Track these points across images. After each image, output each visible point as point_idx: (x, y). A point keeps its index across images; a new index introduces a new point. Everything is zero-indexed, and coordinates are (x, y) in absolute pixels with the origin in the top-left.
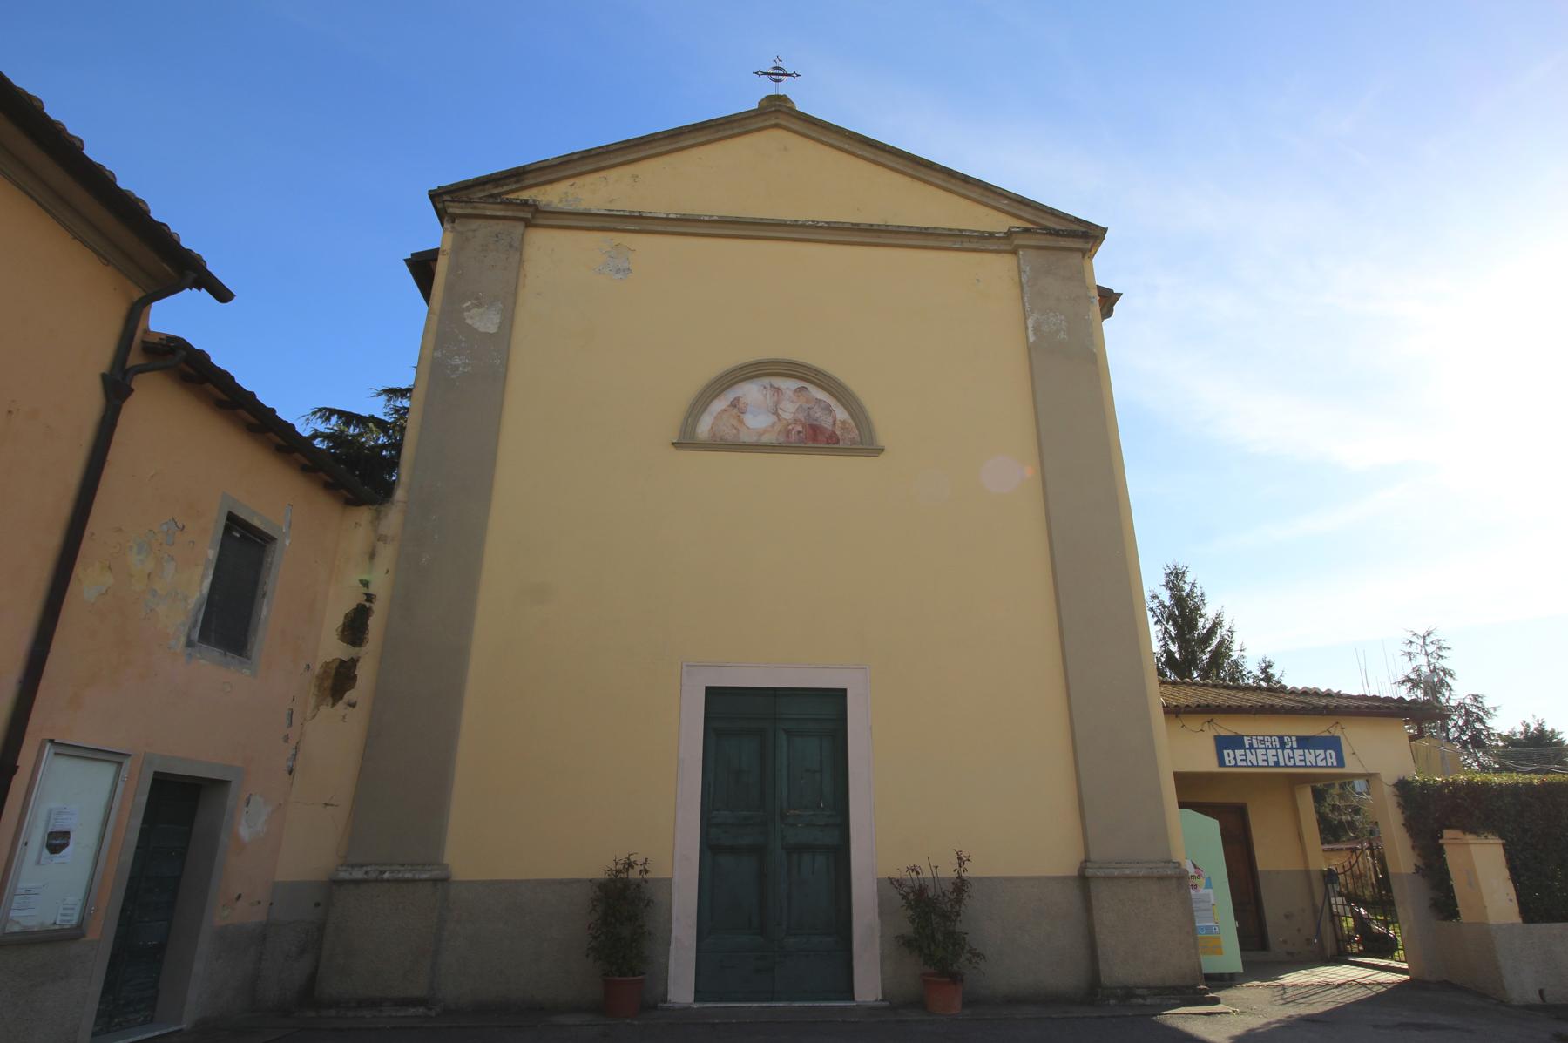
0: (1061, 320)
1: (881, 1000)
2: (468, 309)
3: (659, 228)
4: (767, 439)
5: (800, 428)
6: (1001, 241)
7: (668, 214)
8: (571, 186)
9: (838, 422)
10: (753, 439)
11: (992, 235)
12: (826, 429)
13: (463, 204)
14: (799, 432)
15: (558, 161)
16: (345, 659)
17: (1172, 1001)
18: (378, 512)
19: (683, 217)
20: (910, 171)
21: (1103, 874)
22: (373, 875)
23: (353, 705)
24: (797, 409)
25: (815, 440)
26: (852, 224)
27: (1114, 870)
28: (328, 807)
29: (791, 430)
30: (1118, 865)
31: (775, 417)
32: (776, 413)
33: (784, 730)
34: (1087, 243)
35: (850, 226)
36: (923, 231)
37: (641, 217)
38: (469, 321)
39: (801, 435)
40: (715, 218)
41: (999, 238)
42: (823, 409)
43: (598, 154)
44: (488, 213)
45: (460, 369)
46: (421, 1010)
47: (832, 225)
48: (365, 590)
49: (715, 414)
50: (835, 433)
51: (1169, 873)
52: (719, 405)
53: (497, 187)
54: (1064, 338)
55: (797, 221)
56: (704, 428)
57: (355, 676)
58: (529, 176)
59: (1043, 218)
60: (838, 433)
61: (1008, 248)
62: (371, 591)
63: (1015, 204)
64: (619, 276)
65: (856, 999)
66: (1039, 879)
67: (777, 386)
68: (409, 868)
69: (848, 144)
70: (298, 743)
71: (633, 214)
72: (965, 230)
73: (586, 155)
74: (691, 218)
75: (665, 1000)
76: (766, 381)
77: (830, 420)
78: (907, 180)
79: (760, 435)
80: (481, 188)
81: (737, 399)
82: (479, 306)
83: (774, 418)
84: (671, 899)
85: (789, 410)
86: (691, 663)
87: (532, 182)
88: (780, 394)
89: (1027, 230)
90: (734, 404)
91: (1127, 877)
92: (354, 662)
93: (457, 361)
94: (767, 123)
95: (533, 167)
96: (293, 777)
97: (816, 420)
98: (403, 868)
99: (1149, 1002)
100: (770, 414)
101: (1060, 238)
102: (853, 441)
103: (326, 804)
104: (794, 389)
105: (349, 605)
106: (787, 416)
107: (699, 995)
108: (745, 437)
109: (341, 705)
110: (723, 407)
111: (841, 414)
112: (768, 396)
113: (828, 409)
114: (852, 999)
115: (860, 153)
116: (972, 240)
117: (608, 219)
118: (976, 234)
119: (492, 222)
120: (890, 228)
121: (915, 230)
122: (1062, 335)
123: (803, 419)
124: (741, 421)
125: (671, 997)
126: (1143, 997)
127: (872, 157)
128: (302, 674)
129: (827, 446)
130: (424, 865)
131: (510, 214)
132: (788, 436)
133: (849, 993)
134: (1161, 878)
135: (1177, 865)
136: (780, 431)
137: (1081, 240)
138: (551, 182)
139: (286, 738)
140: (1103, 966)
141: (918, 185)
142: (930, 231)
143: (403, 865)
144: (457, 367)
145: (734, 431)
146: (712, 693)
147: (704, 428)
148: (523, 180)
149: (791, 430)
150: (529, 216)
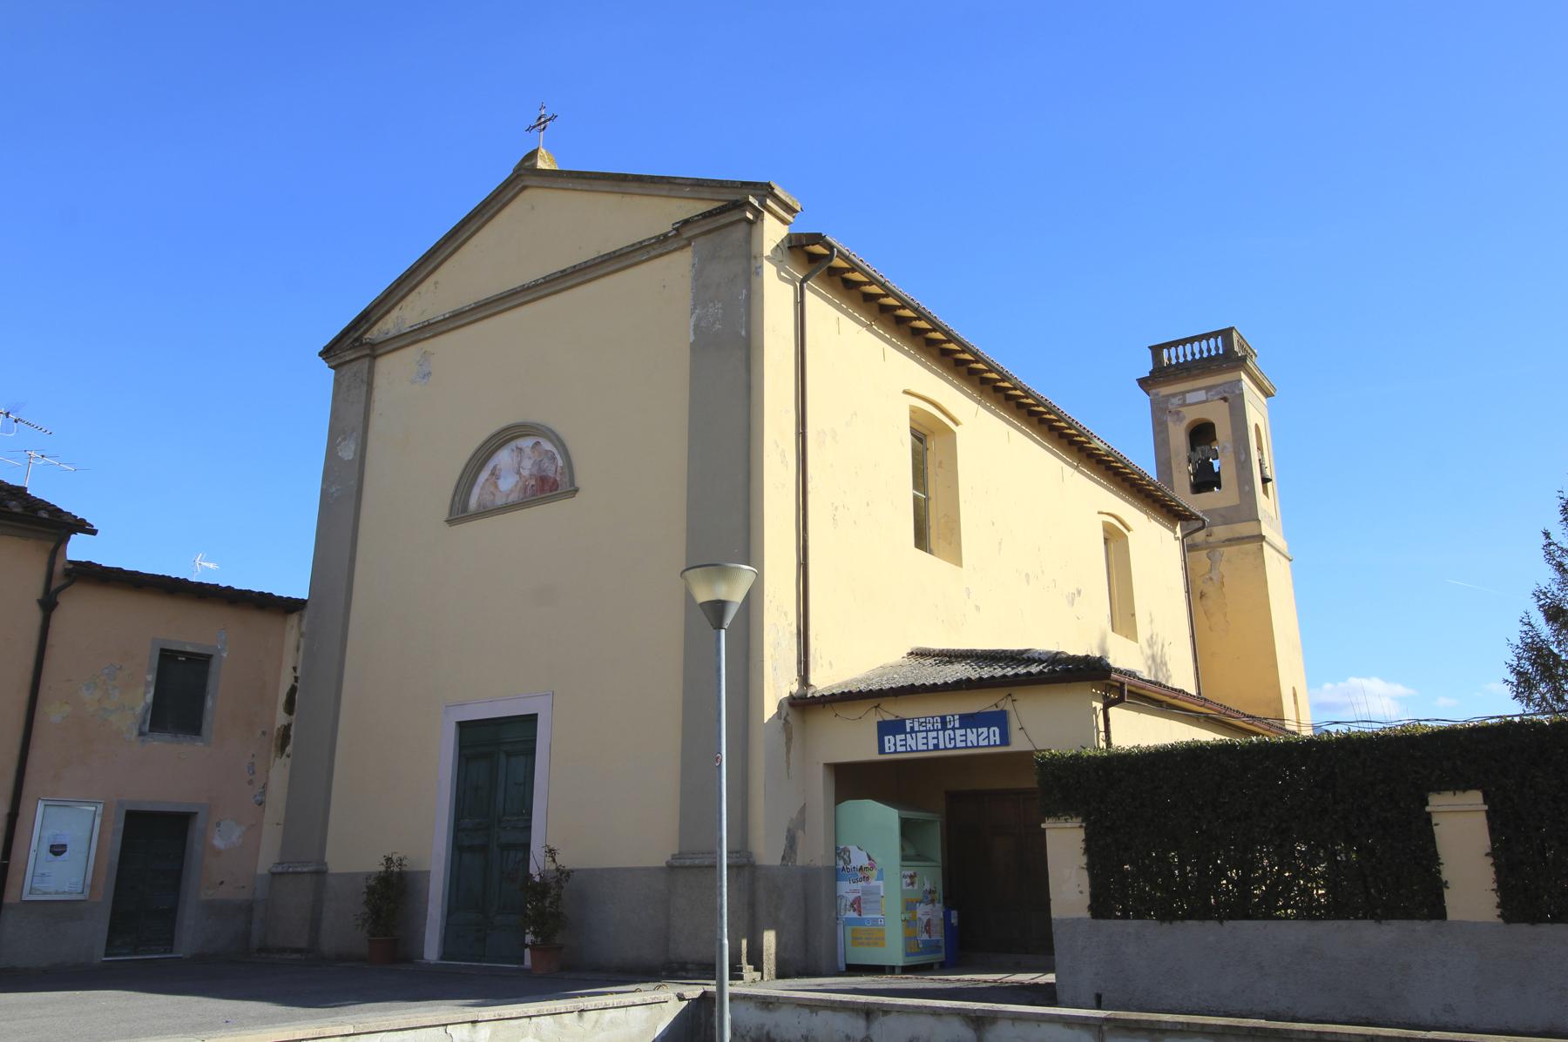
5: (533, 482)
7: (444, 315)
14: (533, 486)
18: (301, 616)
22: (285, 870)
29: (527, 486)
31: (518, 476)
32: (518, 473)
37: (429, 325)
38: (340, 454)
47: (547, 279)
48: (294, 674)
49: (481, 484)
50: (556, 480)
52: (484, 475)
60: (558, 479)
61: (683, 242)
62: (298, 674)
64: (425, 381)
72: (644, 241)
75: (422, 958)
76: (513, 444)
79: (508, 495)
81: (495, 467)
82: (344, 439)
85: (528, 466)
87: (374, 319)
90: (493, 474)
94: (517, 188)
101: (718, 217)
106: (525, 473)
108: (500, 501)
109: (284, 756)
113: (553, 458)
118: (653, 241)
119: (353, 364)
120: (589, 264)
122: (718, 326)
123: (536, 472)
124: (496, 486)
125: (426, 956)
131: (358, 354)
138: (388, 312)
142: (617, 254)
143: (299, 863)
145: (492, 497)
146: (463, 726)
147: (473, 503)
150: (368, 352)
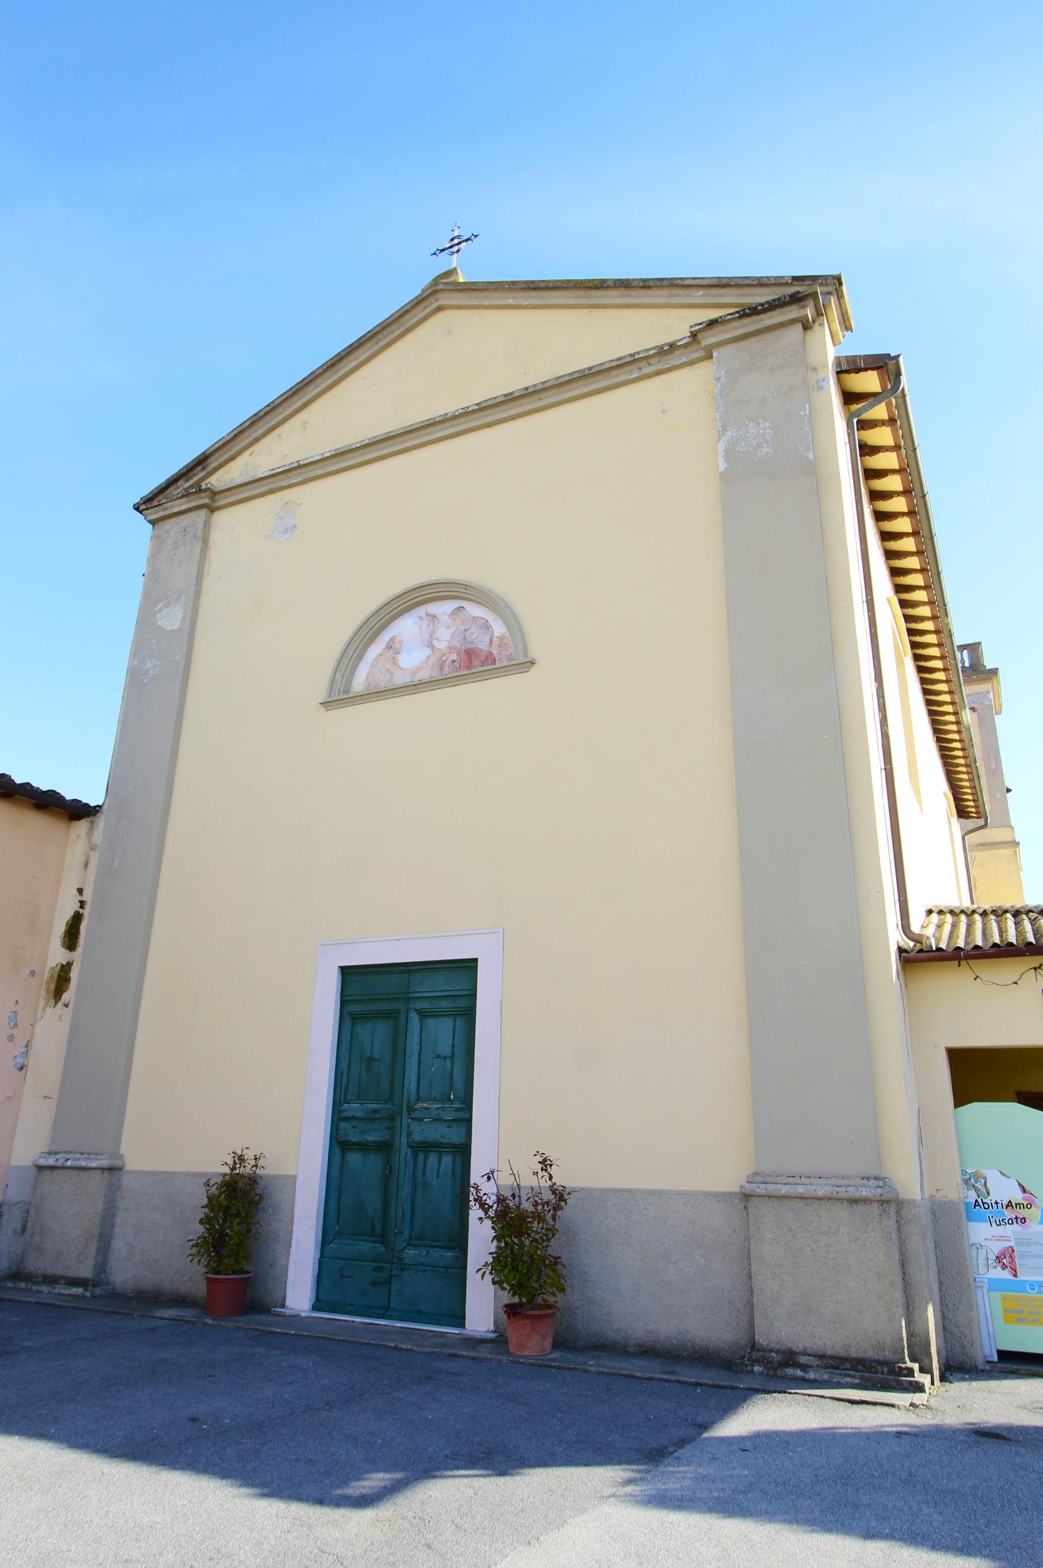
0: (764, 429)
1: (492, 1332)
2: (160, 611)
3: (320, 472)
4: (423, 675)
5: (454, 657)
6: (689, 349)
7: (323, 454)
8: (251, 455)
9: (495, 639)
10: (407, 680)
11: (673, 347)
12: (482, 650)
13: (156, 508)
14: (454, 661)
15: (232, 435)
16: (64, 964)
17: (848, 1379)
18: (92, 822)
19: (337, 452)
20: (584, 301)
21: (764, 1192)
22: (60, 1163)
23: (66, 1006)
24: (452, 635)
25: (469, 667)
26: (505, 396)
27: (779, 1187)
28: (47, 1099)
29: (444, 662)
30: (791, 1180)
31: (430, 649)
32: (431, 645)
33: (416, 1010)
34: (804, 307)
35: (503, 399)
36: (587, 372)
37: (300, 467)
38: (159, 623)
39: (456, 664)
40: (367, 441)
41: (686, 346)
42: (480, 628)
43: (267, 413)
44: (176, 510)
45: (151, 672)
46: (80, 1291)
47: (484, 405)
48: (80, 898)
49: (370, 661)
50: (491, 653)
51: (864, 1193)
52: (375, 650)
53: (187, 481)
54: (768, 453)
55: (446, 414)
56: (359, 682)
57: (70, 978)
58: (212, 459)
59: (752, 295)
60: (495, 652)
61: (701, 353)
62: (84, 898)
63: (713, 291)
64: (287, 536)
65: (467, 1326)
66: (692, 1194)
67: (432, 614)
68: (87, 1156)
69: (513, 298)
70: (28, 1042)
71: (292, 466)
72: (638, 353)
73: (255, 420)
74: (344, 450)
75: (283, 1306)
76: (421, 610)
77: (487, 639)
78: (584, 312)
79: (414, 673)
80: (175, 486)
81: (393, 639)
82: (167, 606)
83: (429, 651)
84: (294, 1197)
85: (445, 638)
86: (325, 943)
87: (214, 465)
88: (436, 621)
89: (712, 323)
90: (389, 647)
91: (802, 1198)
92: (69, 965)
93: (149, 665)
94: (429, 310)
95: (212, 450)
96: (26, 1074)
97: (472, 643)
98: (82, 1157)
99: (811, 1375)
100: (425, 648)
101: (762, 316)
102: (510, 658)
103: (46, 1097)
104: (450, 612)
105: (68, 915)
106: (442, 645)
107: (318, 1304)
108: (399, 680)
109: (60, 1005)
110: (379, 652)
111: (499, 629)
112: (424, 626)
113: (487, 626)
114: (462, 1325)
115: (526, 303)
116: (651, 361)
117: (276, 478)
118: (651, 352)
119: (182, 517)
120: (547, 385)
121: (578, 375)
122: (765, 450)
123: (458, 645)
124: (395, 663)
125: (288, 1303)
126: (804, 1368)
127: (539, 302)
128: (25, 980)
129: (470, 672)
130: (97, 1154)
131: (192, 504)
132: (441, 669)
133: (459, 1319)
134: (854, 1201)
135: (881, 1183)
136: (434, 665)
137: (794, 307)
138: (233, 458)
139: (11, 1038)
140: (757, 1321)
141: (597, 313)
142: (594, 370)
143: (82, 1154)
144: (148, 670)
145: (389, 676)
146: (346, 972)
147: (359, 682)
148: (208, 466)
149: (444, 662)
150: (206, 501)
